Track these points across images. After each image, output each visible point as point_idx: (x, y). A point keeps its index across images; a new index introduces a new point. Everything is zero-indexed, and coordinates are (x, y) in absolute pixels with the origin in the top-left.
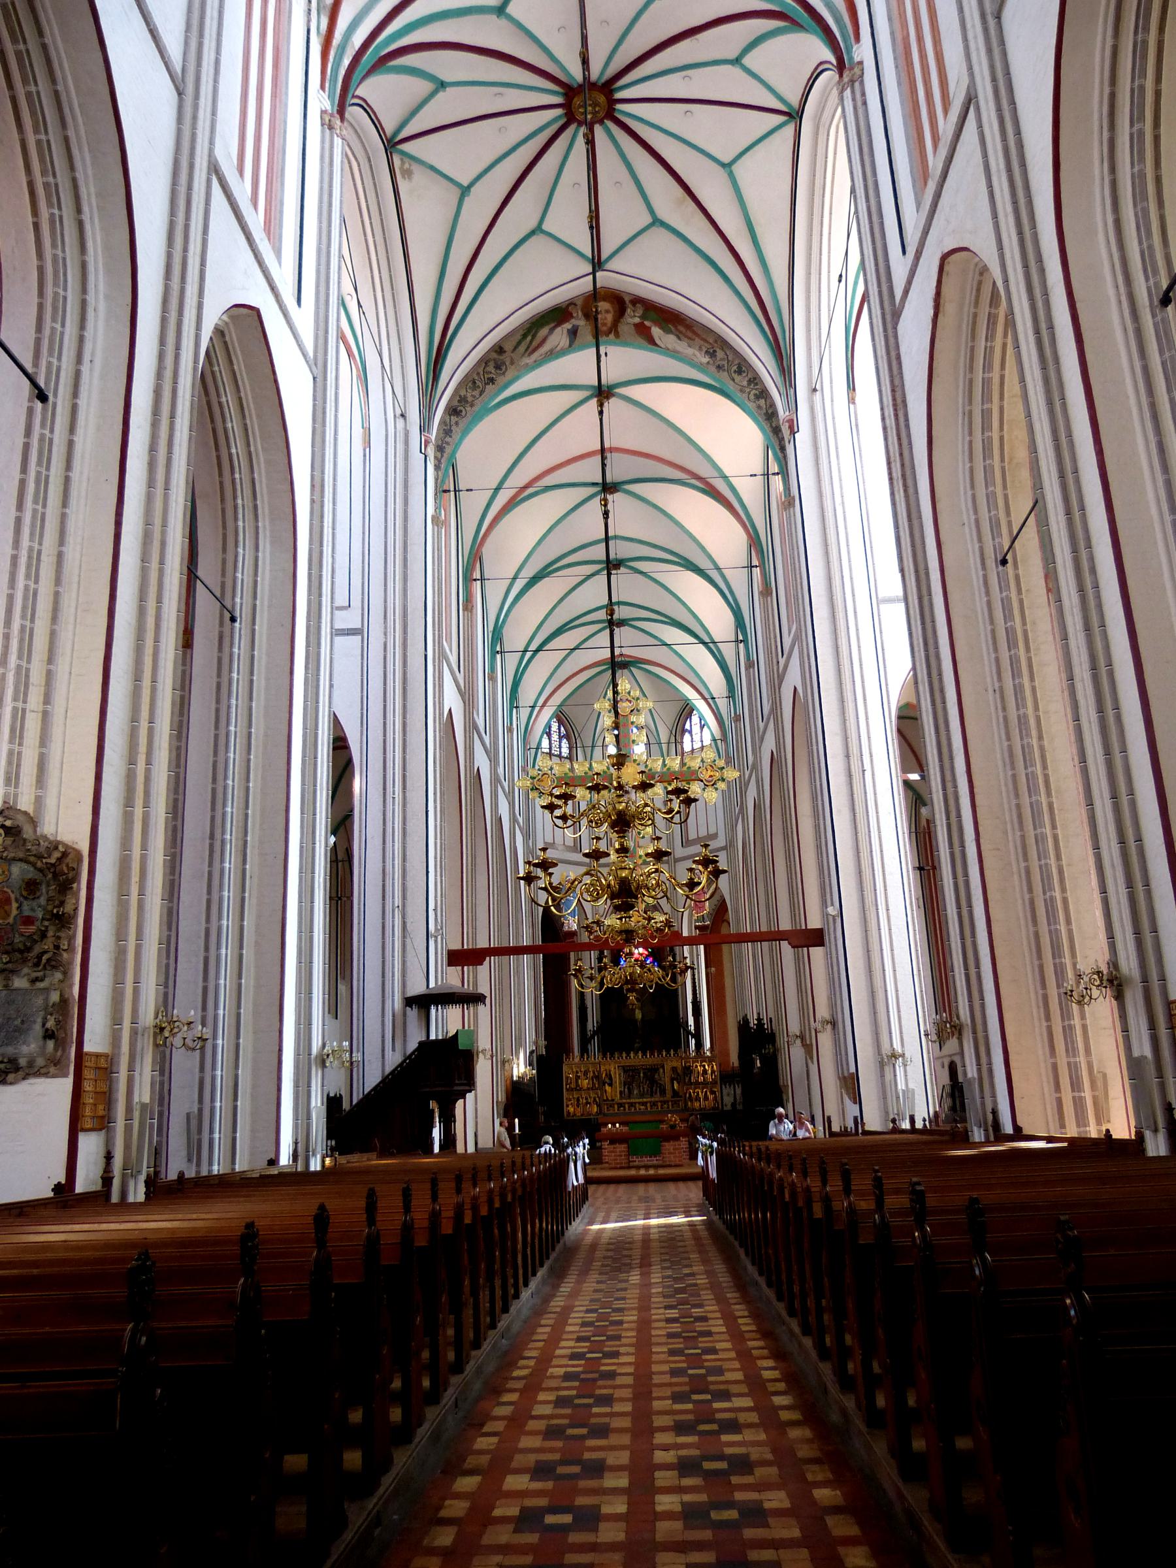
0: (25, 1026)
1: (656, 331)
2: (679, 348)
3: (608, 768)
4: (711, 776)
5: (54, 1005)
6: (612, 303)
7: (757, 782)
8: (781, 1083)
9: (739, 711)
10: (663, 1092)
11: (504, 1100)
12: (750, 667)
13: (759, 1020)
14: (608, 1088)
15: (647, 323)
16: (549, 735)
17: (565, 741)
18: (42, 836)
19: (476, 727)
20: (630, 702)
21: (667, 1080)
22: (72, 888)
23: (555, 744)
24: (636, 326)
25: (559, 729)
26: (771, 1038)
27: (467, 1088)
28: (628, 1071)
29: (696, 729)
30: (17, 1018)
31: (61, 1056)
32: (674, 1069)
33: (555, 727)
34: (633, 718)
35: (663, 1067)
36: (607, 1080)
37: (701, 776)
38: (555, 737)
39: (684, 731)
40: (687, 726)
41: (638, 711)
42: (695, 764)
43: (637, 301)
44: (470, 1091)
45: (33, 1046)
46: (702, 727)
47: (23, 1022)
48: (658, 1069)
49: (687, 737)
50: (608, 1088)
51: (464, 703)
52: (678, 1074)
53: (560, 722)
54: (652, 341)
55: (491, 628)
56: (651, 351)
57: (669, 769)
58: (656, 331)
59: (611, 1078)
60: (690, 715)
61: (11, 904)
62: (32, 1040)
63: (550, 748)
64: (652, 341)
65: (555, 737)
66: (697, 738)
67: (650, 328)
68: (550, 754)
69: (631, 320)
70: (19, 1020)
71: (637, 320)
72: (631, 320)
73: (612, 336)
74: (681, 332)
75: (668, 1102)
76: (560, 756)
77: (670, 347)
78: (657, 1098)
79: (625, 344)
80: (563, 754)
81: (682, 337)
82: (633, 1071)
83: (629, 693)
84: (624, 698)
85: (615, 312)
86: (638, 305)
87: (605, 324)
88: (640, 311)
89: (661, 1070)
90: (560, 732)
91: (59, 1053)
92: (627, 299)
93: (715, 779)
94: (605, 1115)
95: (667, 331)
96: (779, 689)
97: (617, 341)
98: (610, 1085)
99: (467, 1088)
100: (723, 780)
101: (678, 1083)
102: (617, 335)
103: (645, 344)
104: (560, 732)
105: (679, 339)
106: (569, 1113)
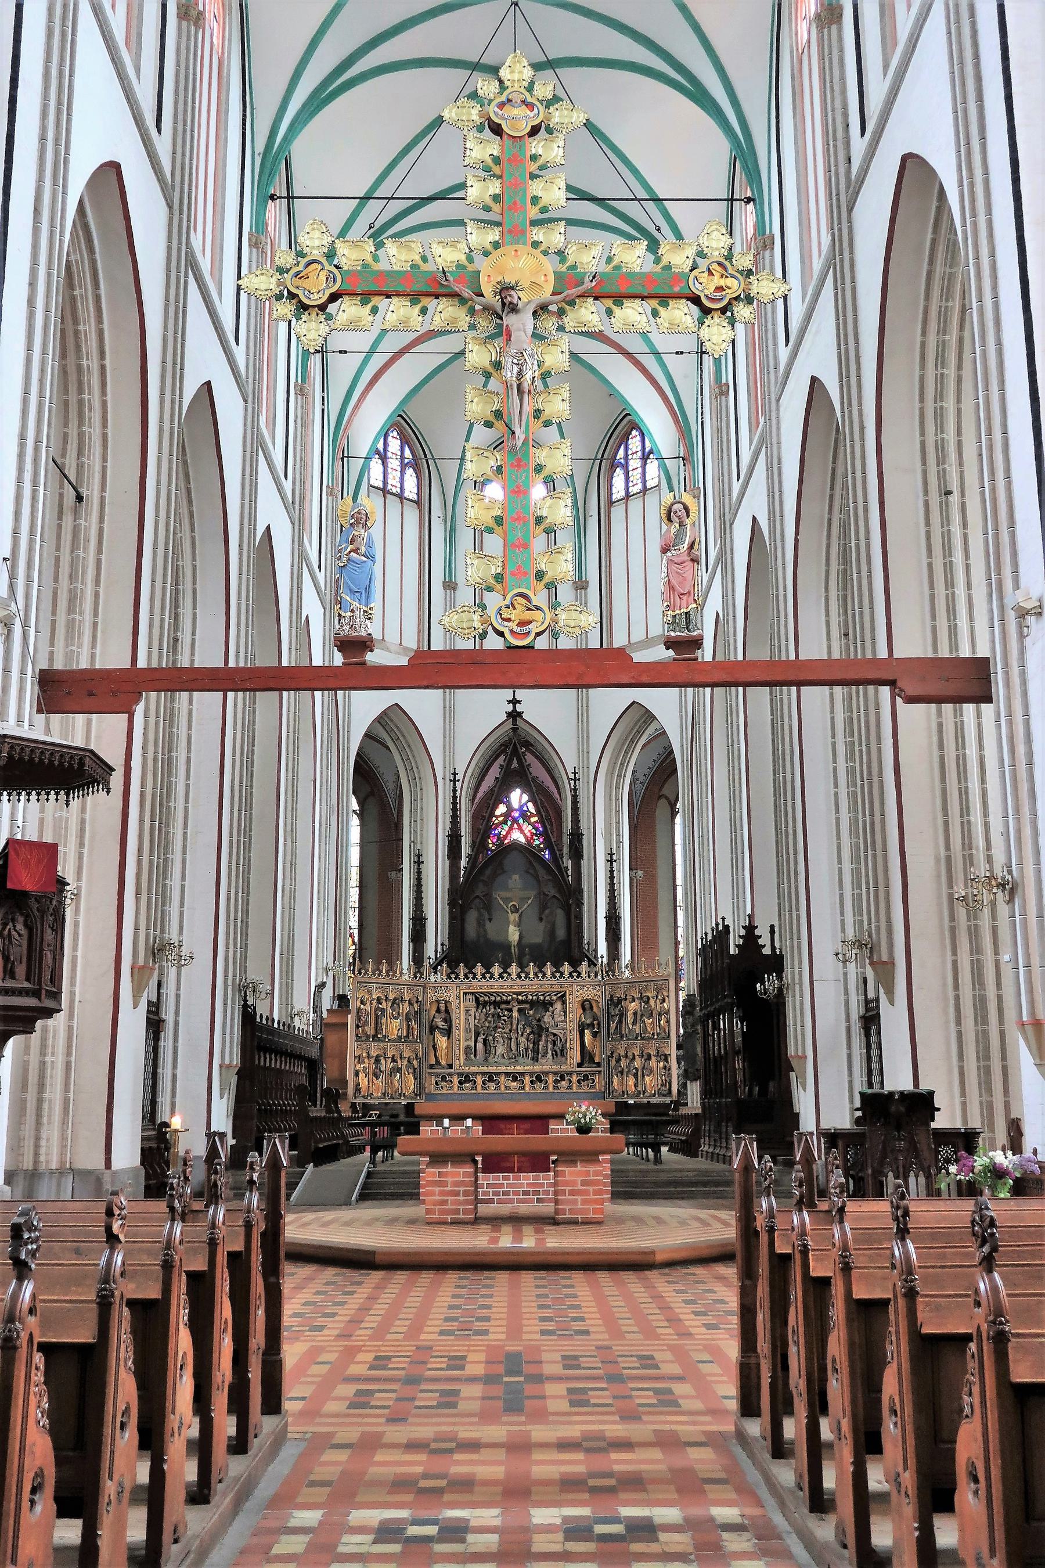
3: (470, 259)
4: (719, 289)
7: (769, 467)
8: (791, 1051)
9: (728, 377)
10: (561, 1053)
11: (236, 1061)
13: (750, 929)
14: (442, 1041)
16: (384, 458)
17: (410, 472)
19: (192, 264)
20: (531, 106)
21: (572, 1027)
23: (393, 481)
25: (402, 450)
26: (776, 963)
27: (31, 1002)
28: (485, 1004)
29: (635, 463)
32: (586, 1006)
33: (394, 445)
34: (536, 146)
35: (562, 998)
36: (441, 1024)
37: (696, 289)
38: (394, 463)
39: (613, 466)
40: (621, 453)
41: (550, 131)
42: (679, 259)
44: (49, 1013)
46: (645, 458)
48: (551, 1004)
49: (619, 474)
50: (442, 1041)
51: (170, 207)
52: (595, 1018)
53: (404, 440)
55: (260, 147)
57: (617, 268)
59: (448, 1020)
60: (625, 438)
63: (385, 482)
65: (394, 463)
66: (635, 476)
68: (384, 491)
75: (570, 1074)
76: (401, 497)
78: (546, 1065)
80: (406, 494)
82: (497, 1004)
83: (530, 88)
84: (517, 98)
89: (558, 1006)
90: (402, 457)
93: (730, 294)
94: (430, 1097)
96: (850, 210)
98: (448, 1033)
99: (31, 1002)
100: (749, 300)
101: (595, 1035)
104: (402, 457)
106: (357, 1089)
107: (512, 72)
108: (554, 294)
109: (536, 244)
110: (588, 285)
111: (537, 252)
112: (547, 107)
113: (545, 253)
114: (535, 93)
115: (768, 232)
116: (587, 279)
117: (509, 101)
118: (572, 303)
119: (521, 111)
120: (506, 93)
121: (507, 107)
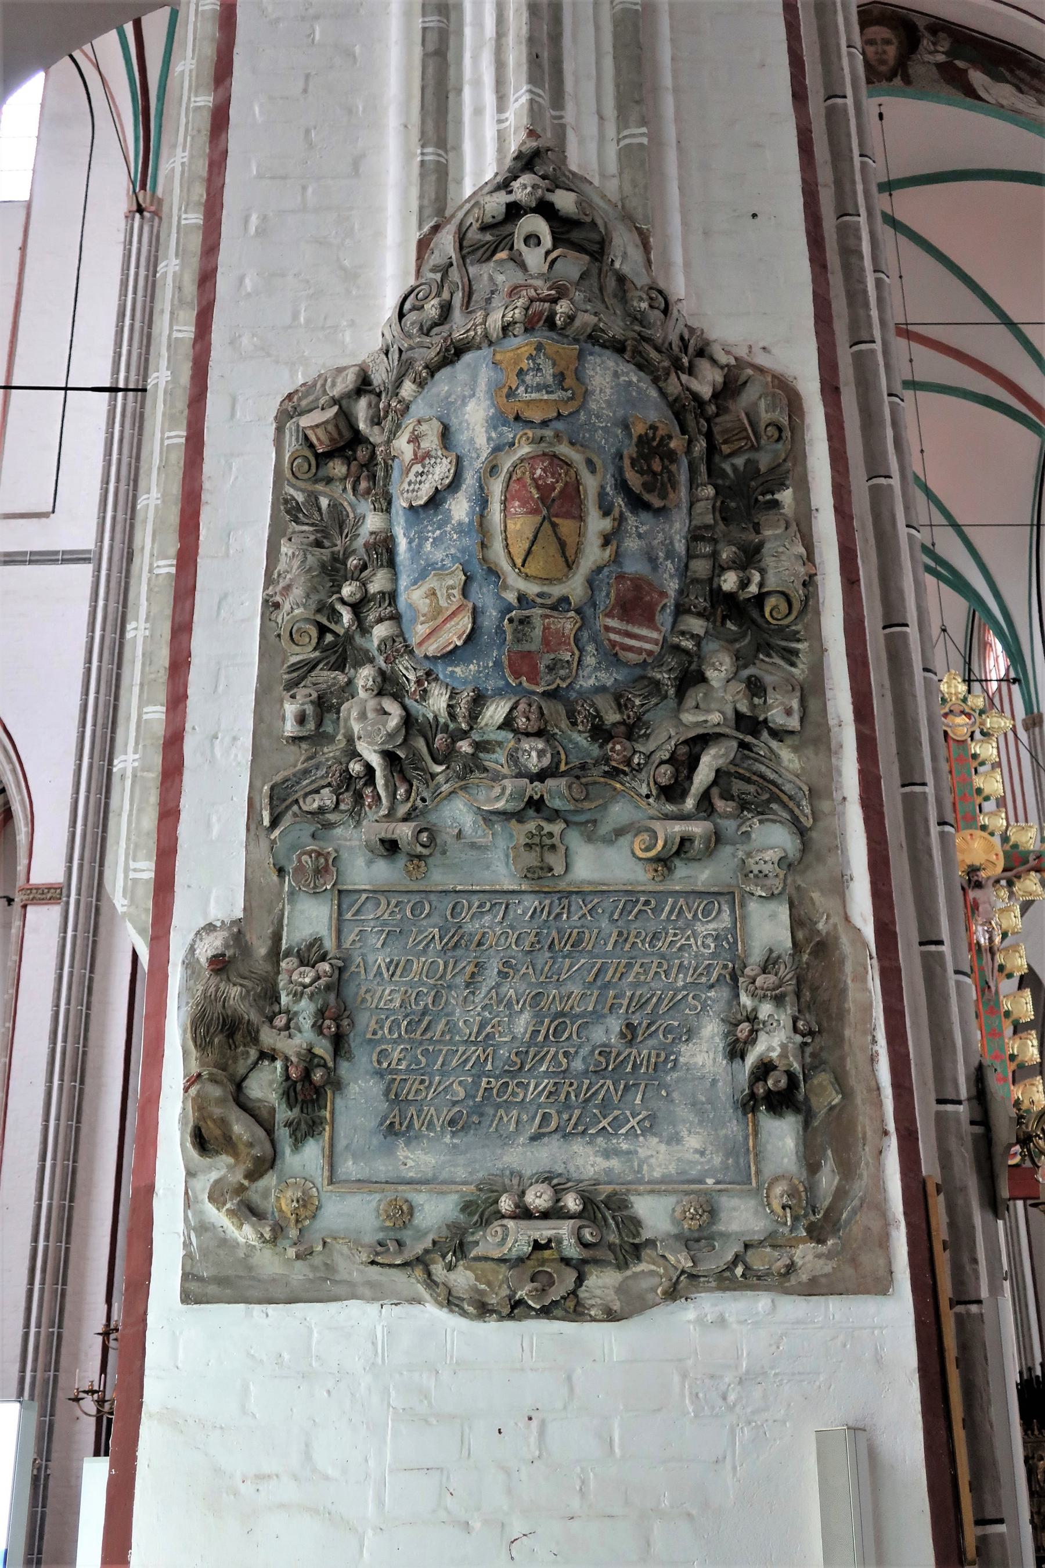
0: (645, 1050)
1: (977, 78)
2: (1020, 106)
5: (768, 965)
6: (893, 28)
12: (1034, 725)
15: (960, 64)
18: (467, 421)
22: (776, 504)
24: (939, 66)
30: (597, 1016)
31: (840, 1194)
43: (940, 27)
45: (693, 1142)
47: (629, 1035)
54: (971, 92)
56: (970, 108)
58: (977, 78)
61: (581, 518)
62: (682, 1111)
64: (971, 92)
67: (966, 71)
69: (928, 58)
70: (615, 1024)
71: (941, 58)
72: (928, 58)
73: (898, 81)
74: (1022, 80)
77: (1004, 102)
79: (921, 96)
81: (1022, 86)
84: (957, 709)
85: (900, 43)
86: (942, 35)
87: (883, 62)
88: (945, 45)
91: (827, 1180)
92: (921, 23)
95: (998, 78)
97: (909, 89)
102: (907, 80)
103: (960, 96)
105: (1021, 91)
107: (949, 687)
108: (1005, 870)
109: (984, 828)
110: (1032, 863)
111: (985, 834)
112: (980, 715)
113: (992, 834)
114: (969, 703)
115: (1036, 710)
116: (1031, 857)
117: (951, 711)
118: (1019, 877)
119: (962, 720)
120: (948, 705)
121: (950, 717)
